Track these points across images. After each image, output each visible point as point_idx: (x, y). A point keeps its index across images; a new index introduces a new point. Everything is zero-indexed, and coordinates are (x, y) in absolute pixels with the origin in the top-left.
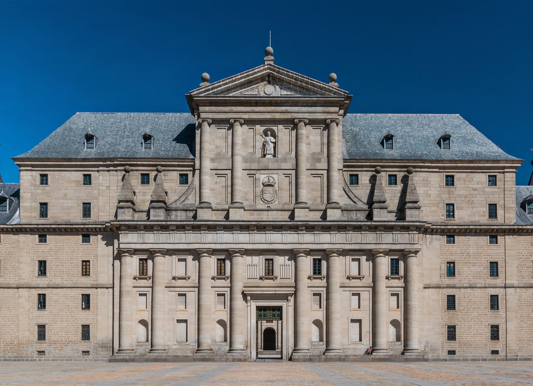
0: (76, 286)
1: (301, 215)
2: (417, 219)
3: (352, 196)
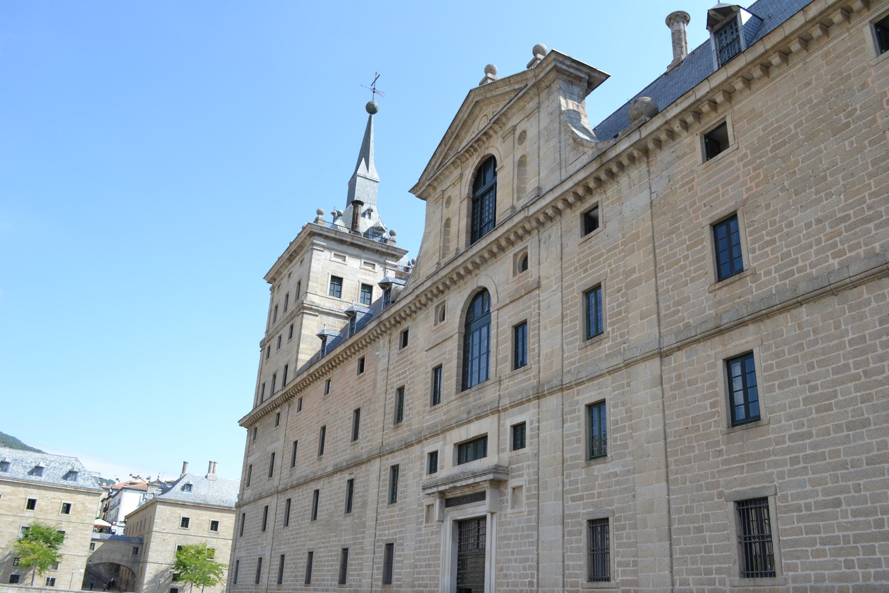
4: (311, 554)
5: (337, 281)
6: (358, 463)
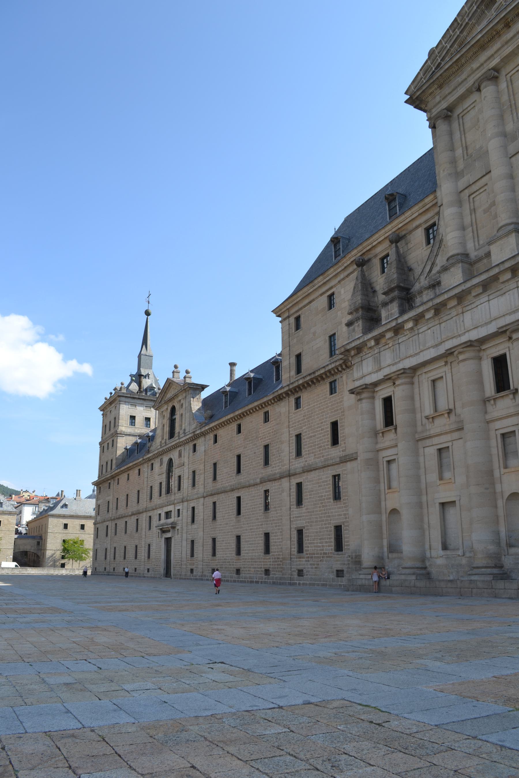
4: (125, 547)
5: (133, 418)
6: (139, 513)
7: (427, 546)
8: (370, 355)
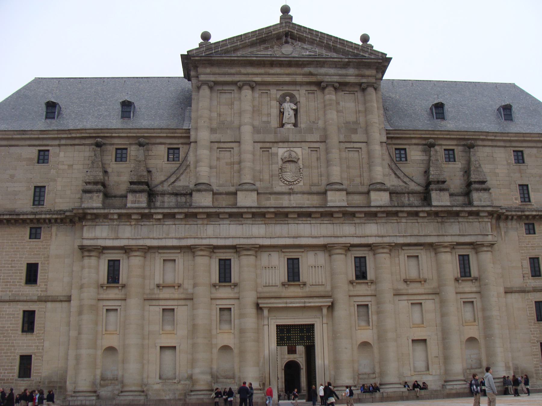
0: (17, 298)
1: (336, 199)
2: (488, 203)
3: (401, 175)
7: (145, 375)
8: (106, 223)
